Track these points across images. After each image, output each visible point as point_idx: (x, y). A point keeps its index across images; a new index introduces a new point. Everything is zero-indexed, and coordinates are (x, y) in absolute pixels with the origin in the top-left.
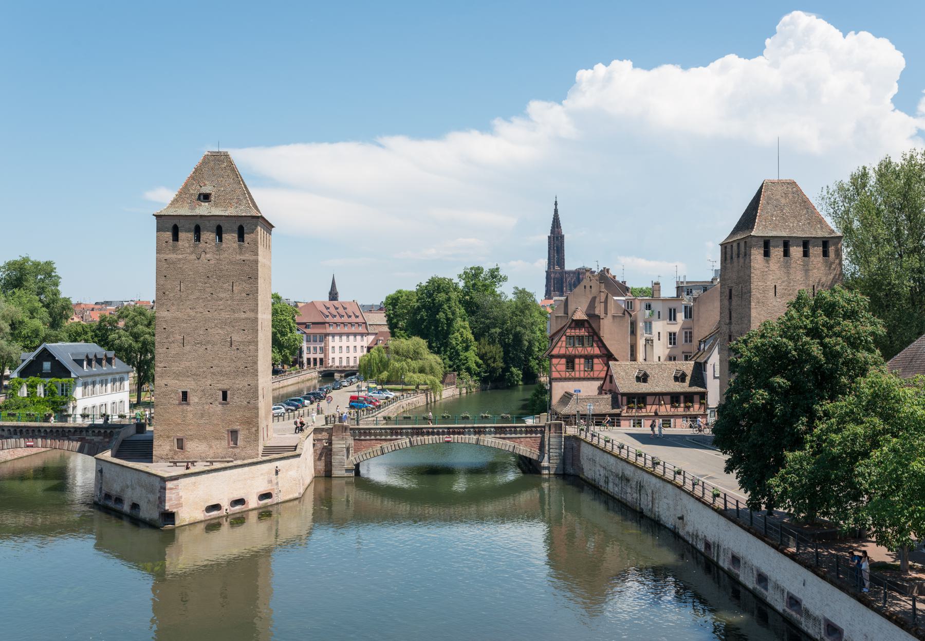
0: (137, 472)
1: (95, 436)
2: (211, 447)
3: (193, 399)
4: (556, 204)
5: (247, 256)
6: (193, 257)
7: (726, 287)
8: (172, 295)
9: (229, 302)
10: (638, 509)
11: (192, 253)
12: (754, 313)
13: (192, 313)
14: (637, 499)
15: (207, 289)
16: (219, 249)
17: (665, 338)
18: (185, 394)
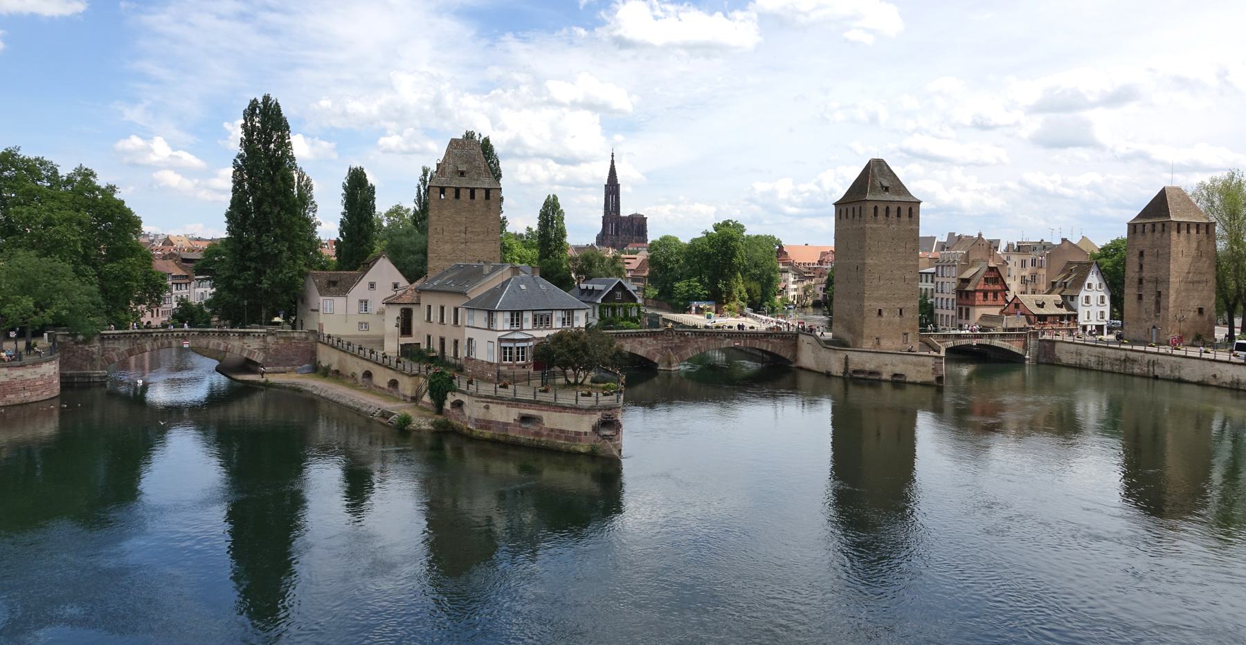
0: (901, 356)
1: (775, 339)
2: (894, 343)
3: (885, 314)
4: (613, 156)
5: (914, 227)
6: (886, 226)
7: (1136, 250)
8: (874, 249)
9: (904, 255)
10: (1151, 375)
11: (885, 223)
12: (1171, 267)
13: (885, 261)
14: (1148, 370)
15: (893, 247)
16: (899, 222)
17: (1018, 280)
18: (880, 310)
